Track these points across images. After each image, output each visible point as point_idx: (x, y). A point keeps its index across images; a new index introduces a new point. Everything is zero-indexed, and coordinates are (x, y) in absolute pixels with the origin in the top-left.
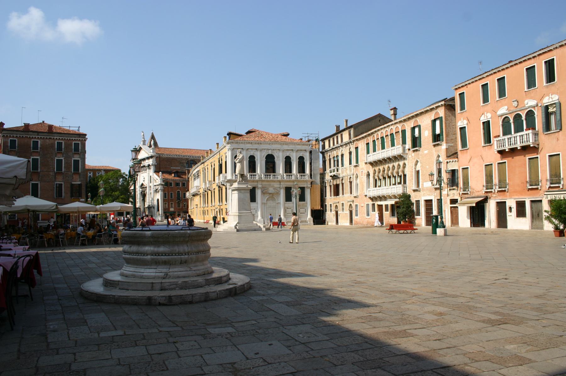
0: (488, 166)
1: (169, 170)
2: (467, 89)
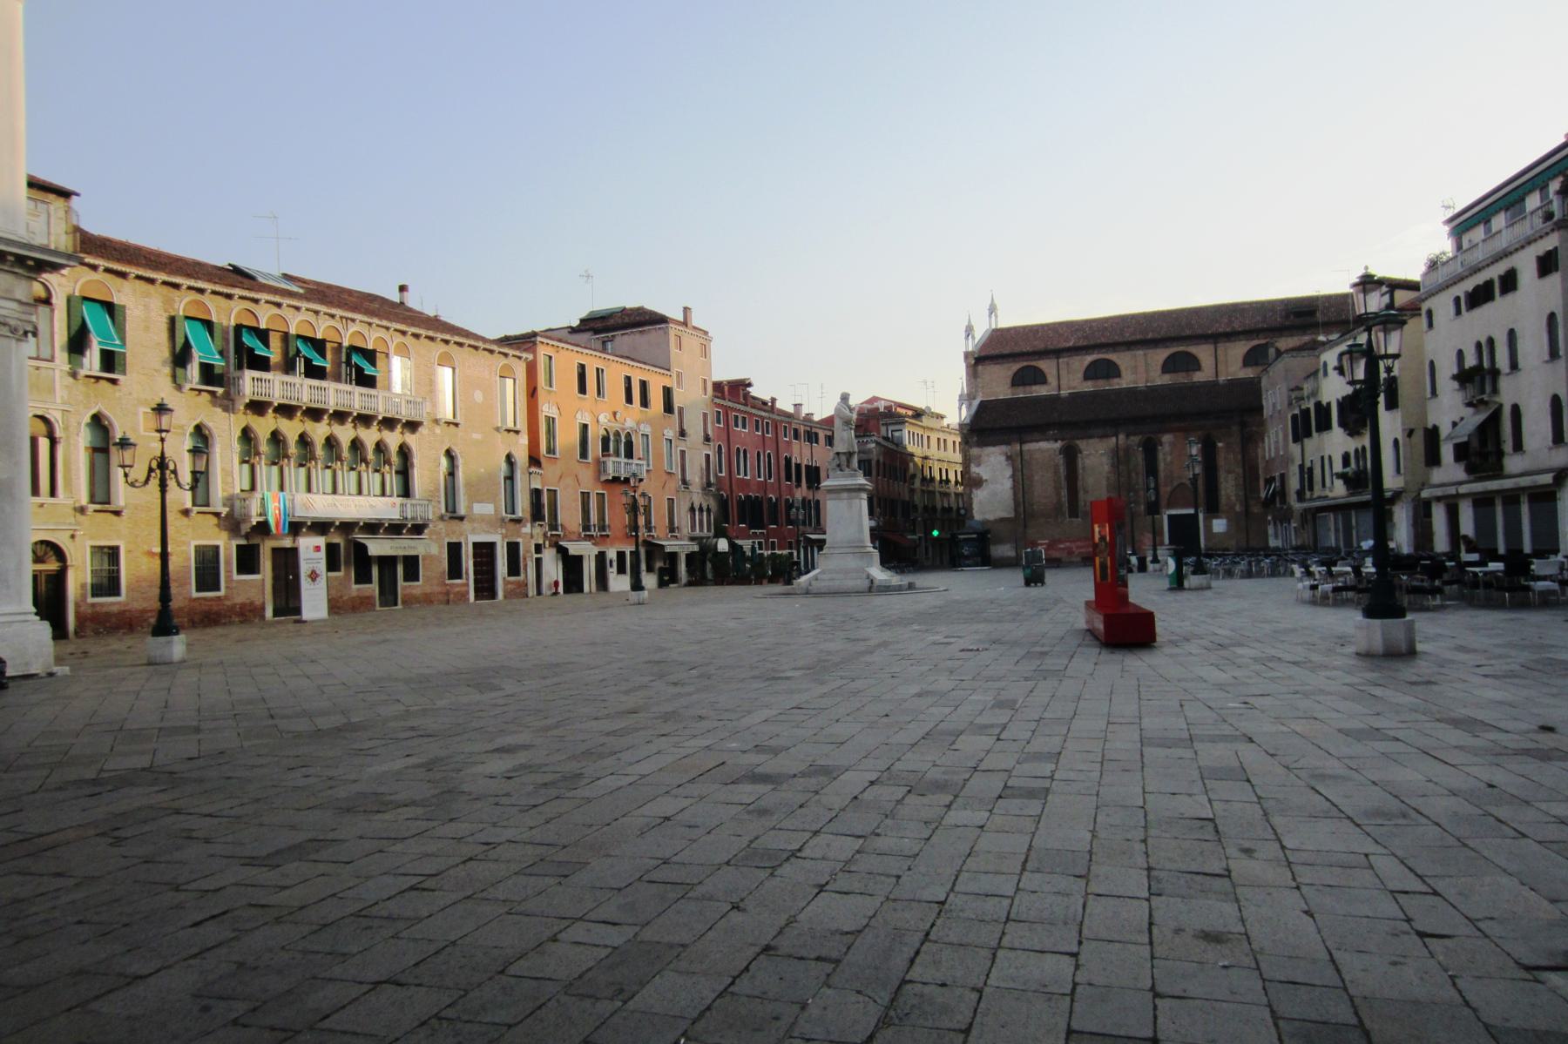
0: (585, 497)
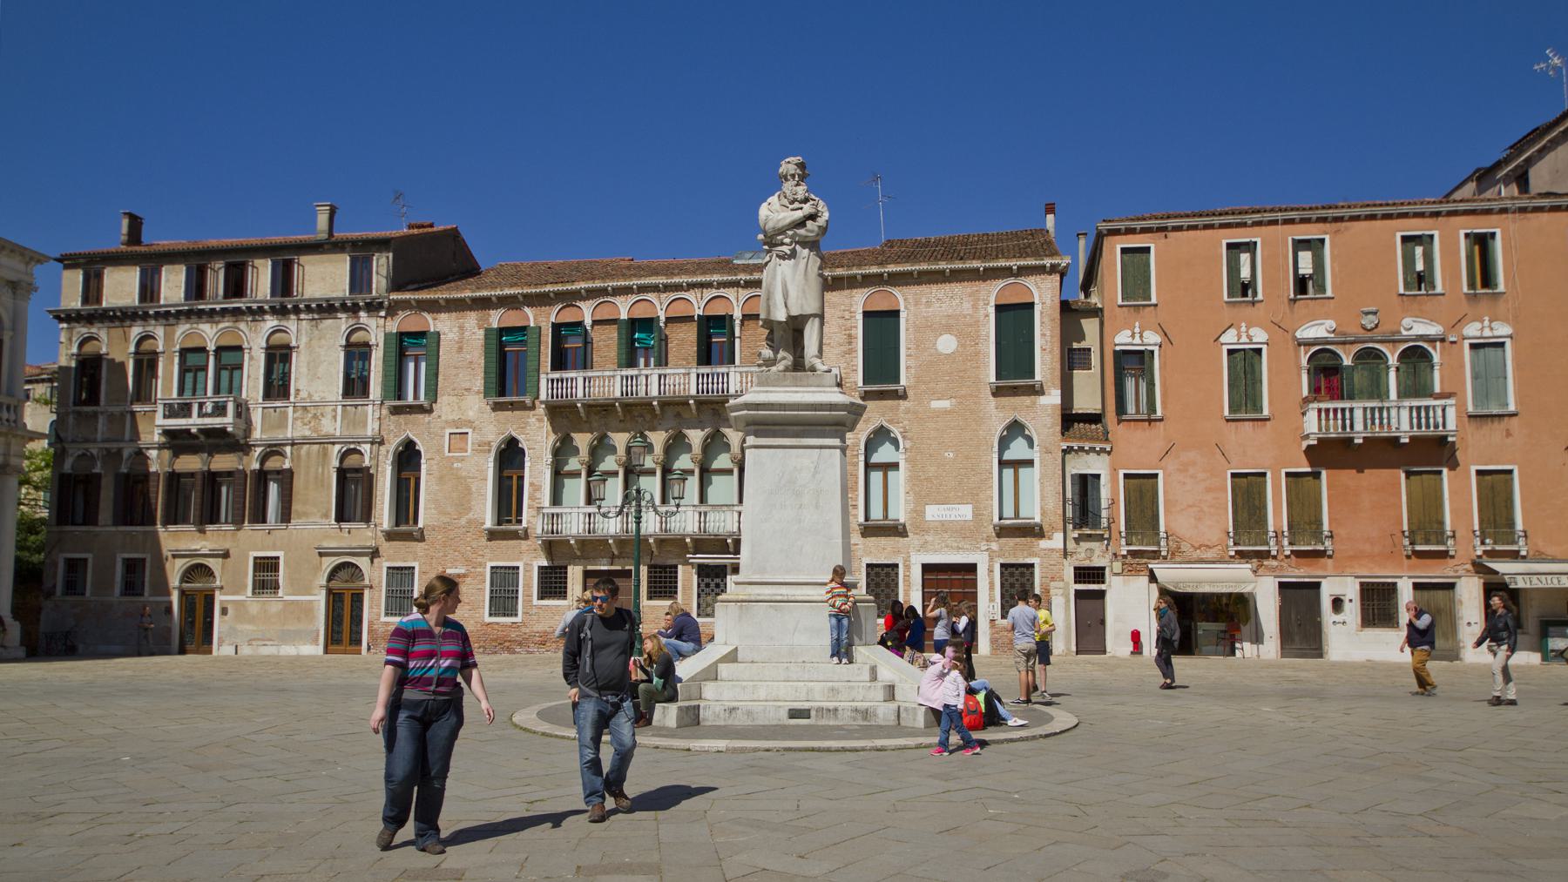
2: (1163, 240)
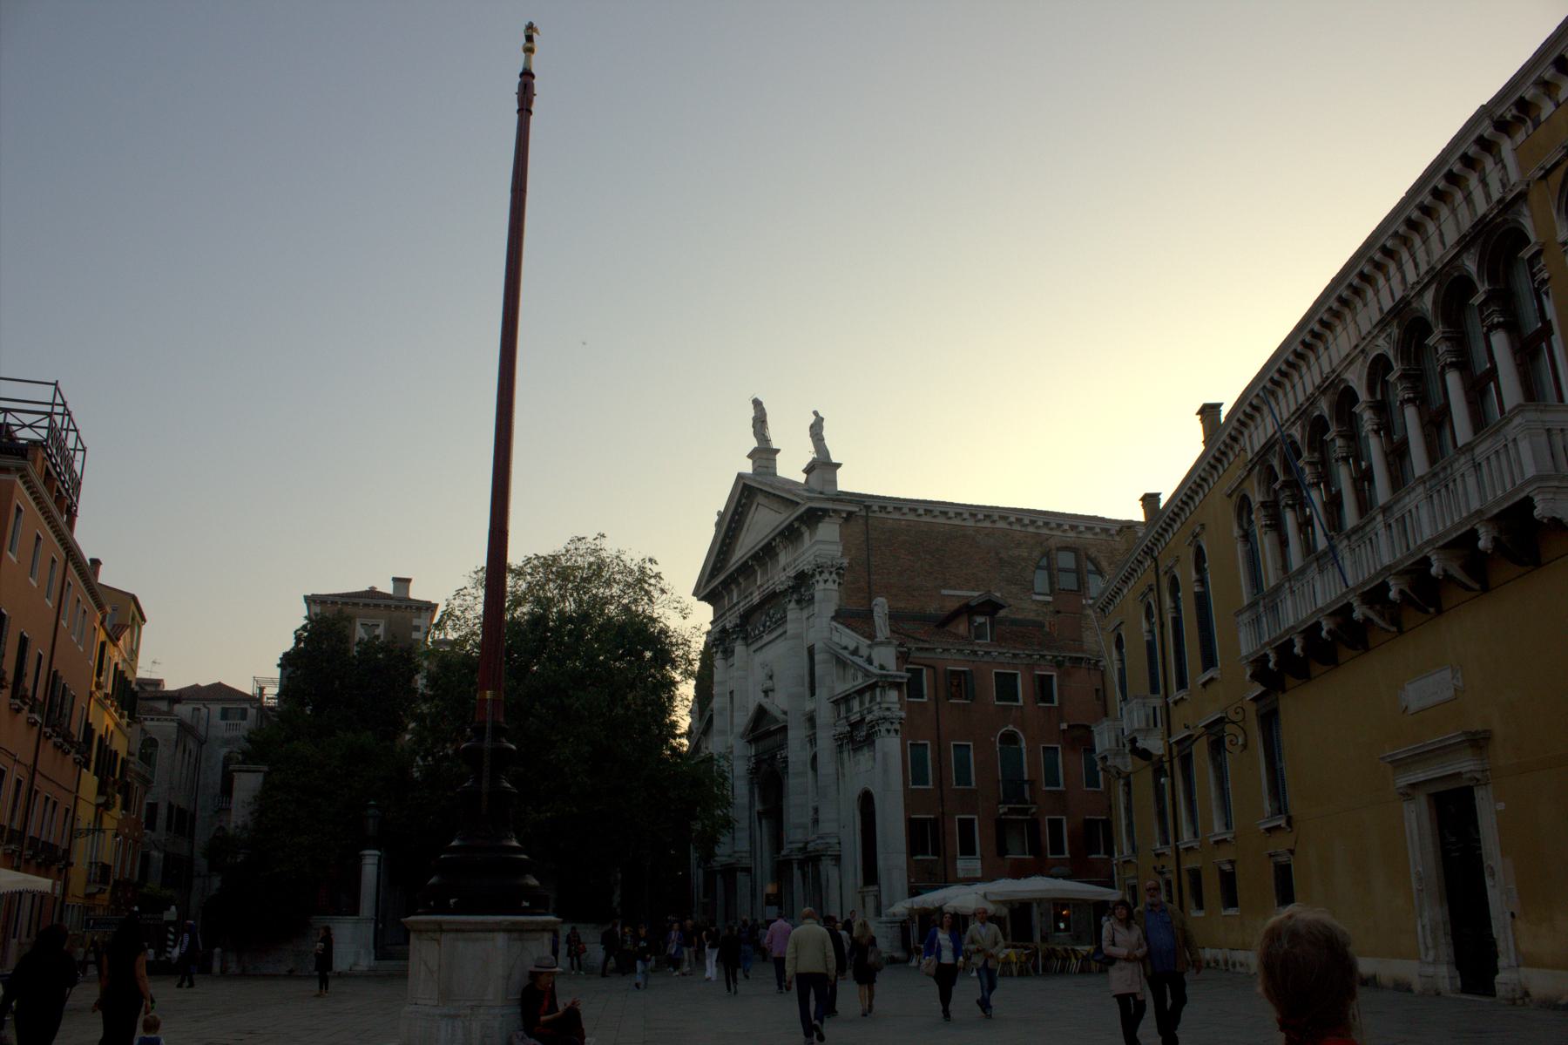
1: (932, 608)
